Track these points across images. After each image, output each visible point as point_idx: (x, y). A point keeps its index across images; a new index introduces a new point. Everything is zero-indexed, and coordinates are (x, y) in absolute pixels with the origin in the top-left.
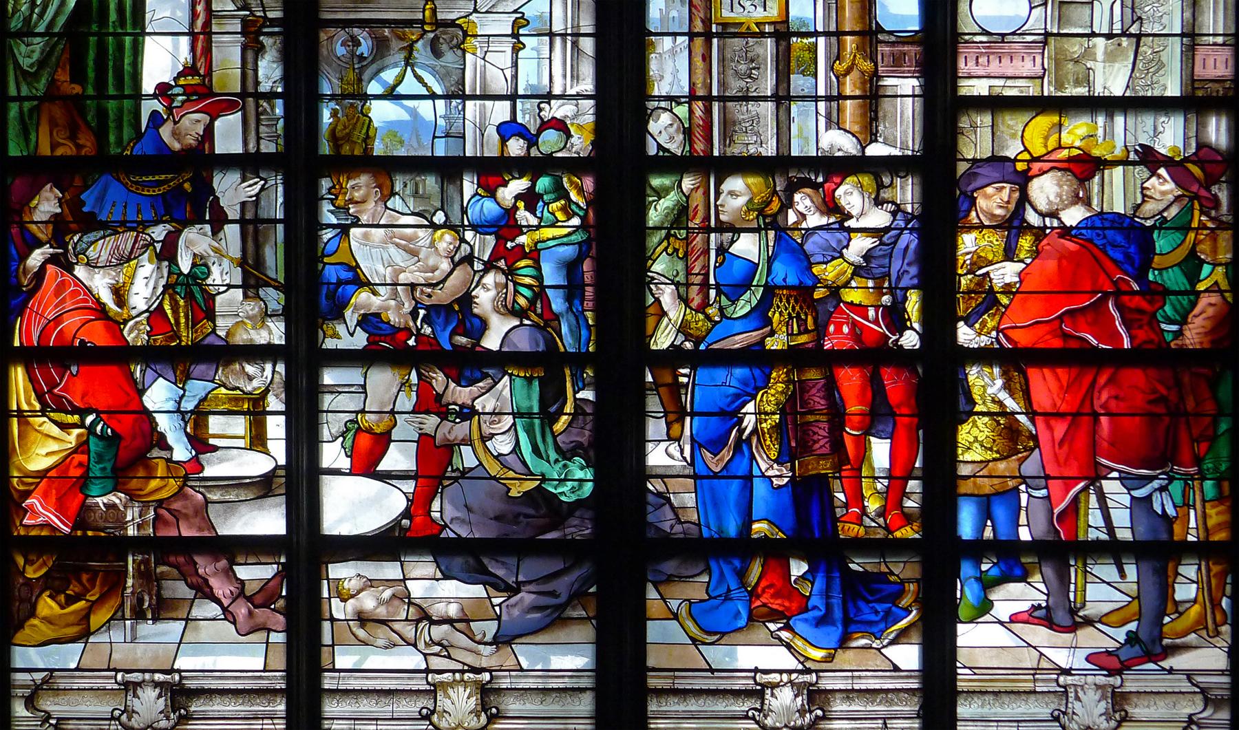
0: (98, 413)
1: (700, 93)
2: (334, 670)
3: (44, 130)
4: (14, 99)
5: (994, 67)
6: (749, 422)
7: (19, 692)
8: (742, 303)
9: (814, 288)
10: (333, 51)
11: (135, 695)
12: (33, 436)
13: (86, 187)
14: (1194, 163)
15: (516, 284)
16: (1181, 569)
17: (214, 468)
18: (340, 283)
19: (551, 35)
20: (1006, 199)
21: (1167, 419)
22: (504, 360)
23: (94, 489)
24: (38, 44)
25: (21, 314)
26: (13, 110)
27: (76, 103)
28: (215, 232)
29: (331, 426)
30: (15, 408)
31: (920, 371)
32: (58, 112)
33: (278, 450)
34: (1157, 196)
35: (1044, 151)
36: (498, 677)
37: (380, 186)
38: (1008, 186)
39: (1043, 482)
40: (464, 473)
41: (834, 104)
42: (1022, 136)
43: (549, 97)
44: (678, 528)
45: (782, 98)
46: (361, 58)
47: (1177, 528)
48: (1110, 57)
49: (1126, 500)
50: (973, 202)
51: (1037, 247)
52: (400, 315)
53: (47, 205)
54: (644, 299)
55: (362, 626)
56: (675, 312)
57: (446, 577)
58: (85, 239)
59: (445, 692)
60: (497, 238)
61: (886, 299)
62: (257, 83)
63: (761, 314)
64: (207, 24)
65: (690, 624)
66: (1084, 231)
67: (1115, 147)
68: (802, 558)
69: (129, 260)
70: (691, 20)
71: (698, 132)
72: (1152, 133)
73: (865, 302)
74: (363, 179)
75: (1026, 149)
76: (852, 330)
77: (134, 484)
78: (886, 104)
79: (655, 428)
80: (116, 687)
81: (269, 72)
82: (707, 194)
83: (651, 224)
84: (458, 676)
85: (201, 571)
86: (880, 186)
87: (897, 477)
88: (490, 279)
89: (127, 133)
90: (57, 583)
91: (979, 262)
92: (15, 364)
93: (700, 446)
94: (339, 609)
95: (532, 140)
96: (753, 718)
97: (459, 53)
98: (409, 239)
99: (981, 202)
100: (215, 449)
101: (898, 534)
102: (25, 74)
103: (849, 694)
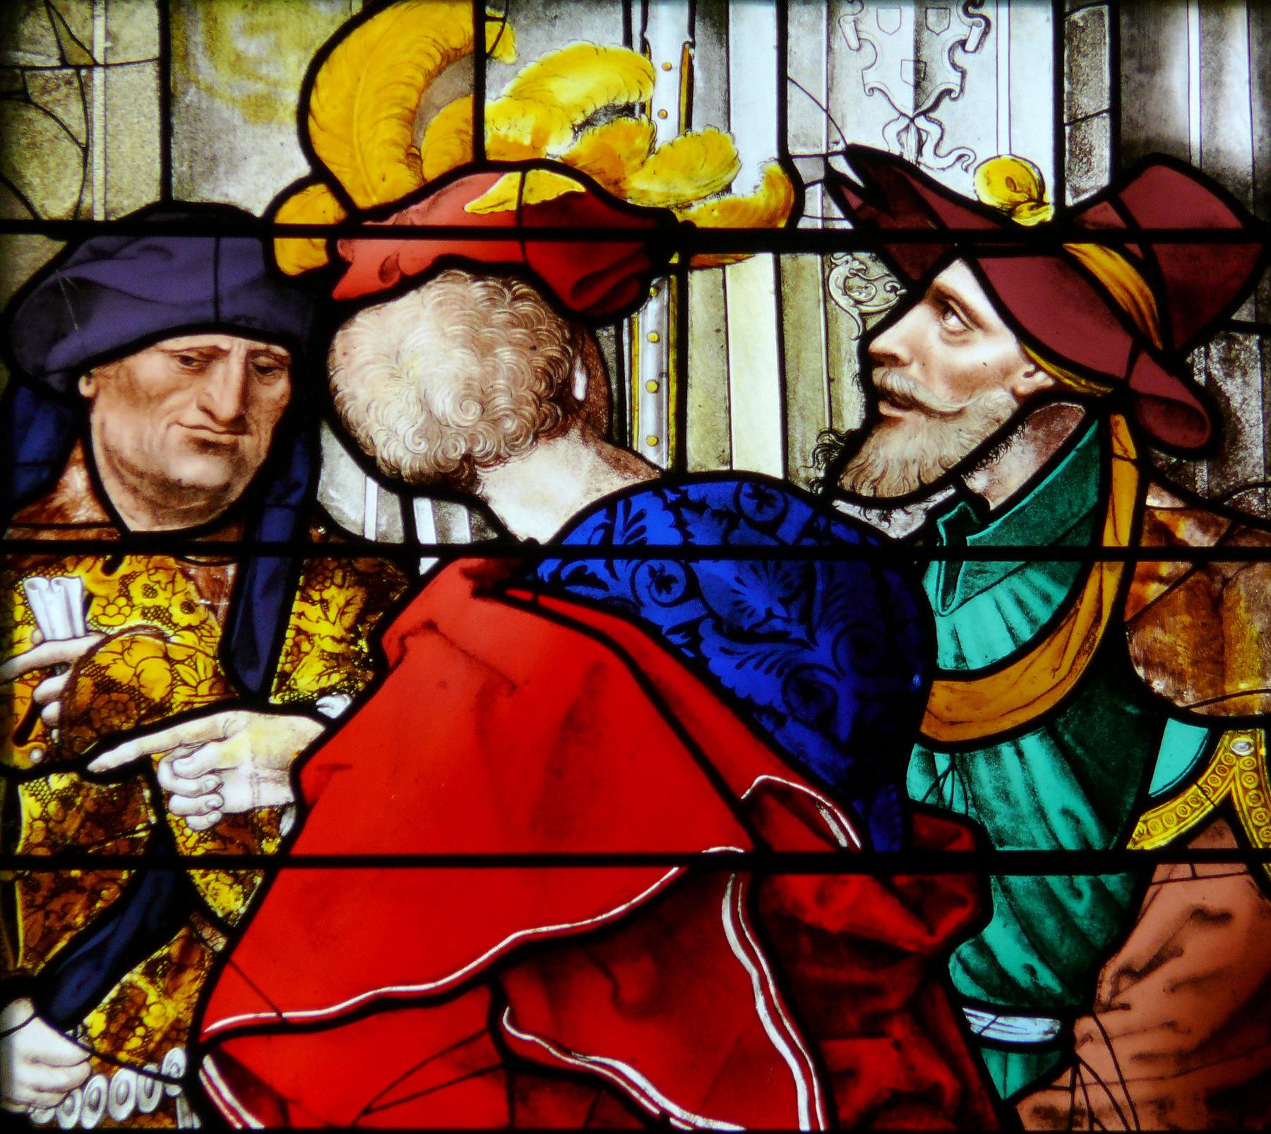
14: (1107, 239)
20: (227, 407)
34: (938, 396)
35: (402, 181)
38: (237, 347)
42: (304, 112)
51: (374, 640)
66: (596, 566)
67: (733, 162)
72: (906, 100)
75: (320, 174)
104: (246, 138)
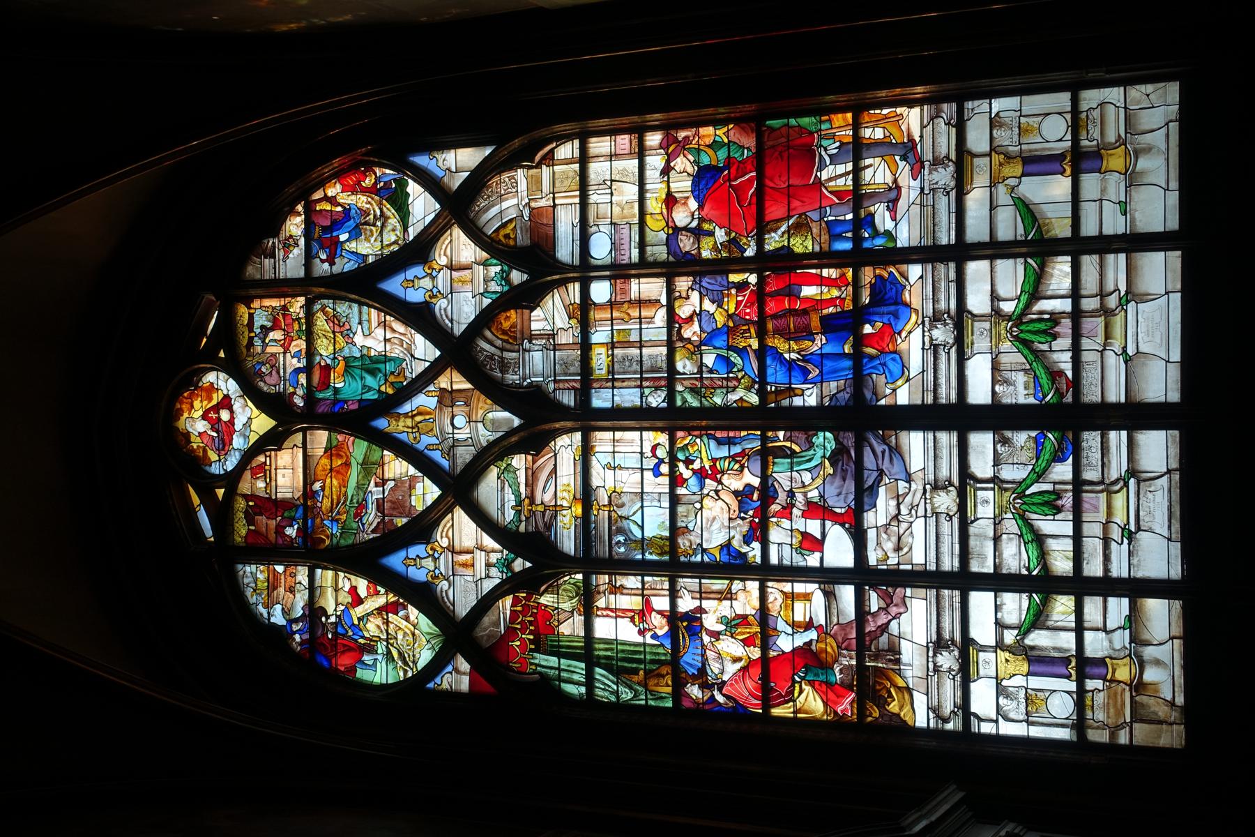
0: (794, 674)
1: (639, 383)
2: (926, 564)
3: (660, 689)
4: (647, 702)
5: (626, 247)
6: (794, 356)
7: (940, 726)
8: (736, 361)
9: (728, 327)
10: (623, 553)
11: (941, 666)
12: (806, 707)
13: (686, 672)
15: (728, 470)
16: (867, 136)
17: (820, 619)
18: (729, 554)
19: (614, 452)
21: (791, 151)
22: (765, 477)
23: (833, 679)
24: (621, 689)
25: (746, 708)
26: (652, 703)
27: (648, 673)
28: (706, 612)
29: (799, 561)
30: (792, 715)
31: (768, 273)
32: (652, 682)
33: (811, 587)
35: (663, 221)
36: (928, 481)
37: (683, 533)
39: (823, 209)
40: (822, 496)
41: (643, 320)
43: (642, 453)
44: (848, 390)
45: (641, 345)
46: (625, 540)
47: (845, 141)
48: (621, 193)
49: (832, 167)
50: (687, 253)
52: (744, 525)
53: (694, 691)
54: (734, 408)
55: (902, 549)
56: (740, 393)
57: (875, 506)
58: (710, 674)
59: (937, 508)
60: (707, 478)
61: (733, 291)
62: (637, 589)
63: (742, 352)
64: (611, 610)
65: (900, 382)
68: (863, 328)
69: (719, 654)
70: (607, 388)
71: (657, 384)
73: (735, 302)
74: (680, 541)
76: (749, 307)
77: (829, 659)
78: (643, 296)
79: (798, 401)
80: (936, 676)
81: (632, 582)
82: (684, 379)
83: (699, 405)
84: (928, 501)
85: (874, 629)
86: (680, 297)
87: (821, 281)
88: (725, 479)
89: (661, 650)
90: (881, 701)
91: (715, 248)
92: (770, 712)
93: (806, 380)
94: (893, 561)
95: (661, 461)
96: (949, 349)
97: (622, 494)
98: (708, 520)
99: (687, 249)
100: (811, 618)
101: (850, 280)
102: (635, 696)
103: (935, 301)
104: (659, 237)
